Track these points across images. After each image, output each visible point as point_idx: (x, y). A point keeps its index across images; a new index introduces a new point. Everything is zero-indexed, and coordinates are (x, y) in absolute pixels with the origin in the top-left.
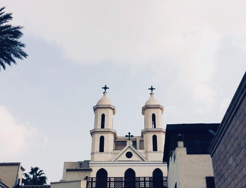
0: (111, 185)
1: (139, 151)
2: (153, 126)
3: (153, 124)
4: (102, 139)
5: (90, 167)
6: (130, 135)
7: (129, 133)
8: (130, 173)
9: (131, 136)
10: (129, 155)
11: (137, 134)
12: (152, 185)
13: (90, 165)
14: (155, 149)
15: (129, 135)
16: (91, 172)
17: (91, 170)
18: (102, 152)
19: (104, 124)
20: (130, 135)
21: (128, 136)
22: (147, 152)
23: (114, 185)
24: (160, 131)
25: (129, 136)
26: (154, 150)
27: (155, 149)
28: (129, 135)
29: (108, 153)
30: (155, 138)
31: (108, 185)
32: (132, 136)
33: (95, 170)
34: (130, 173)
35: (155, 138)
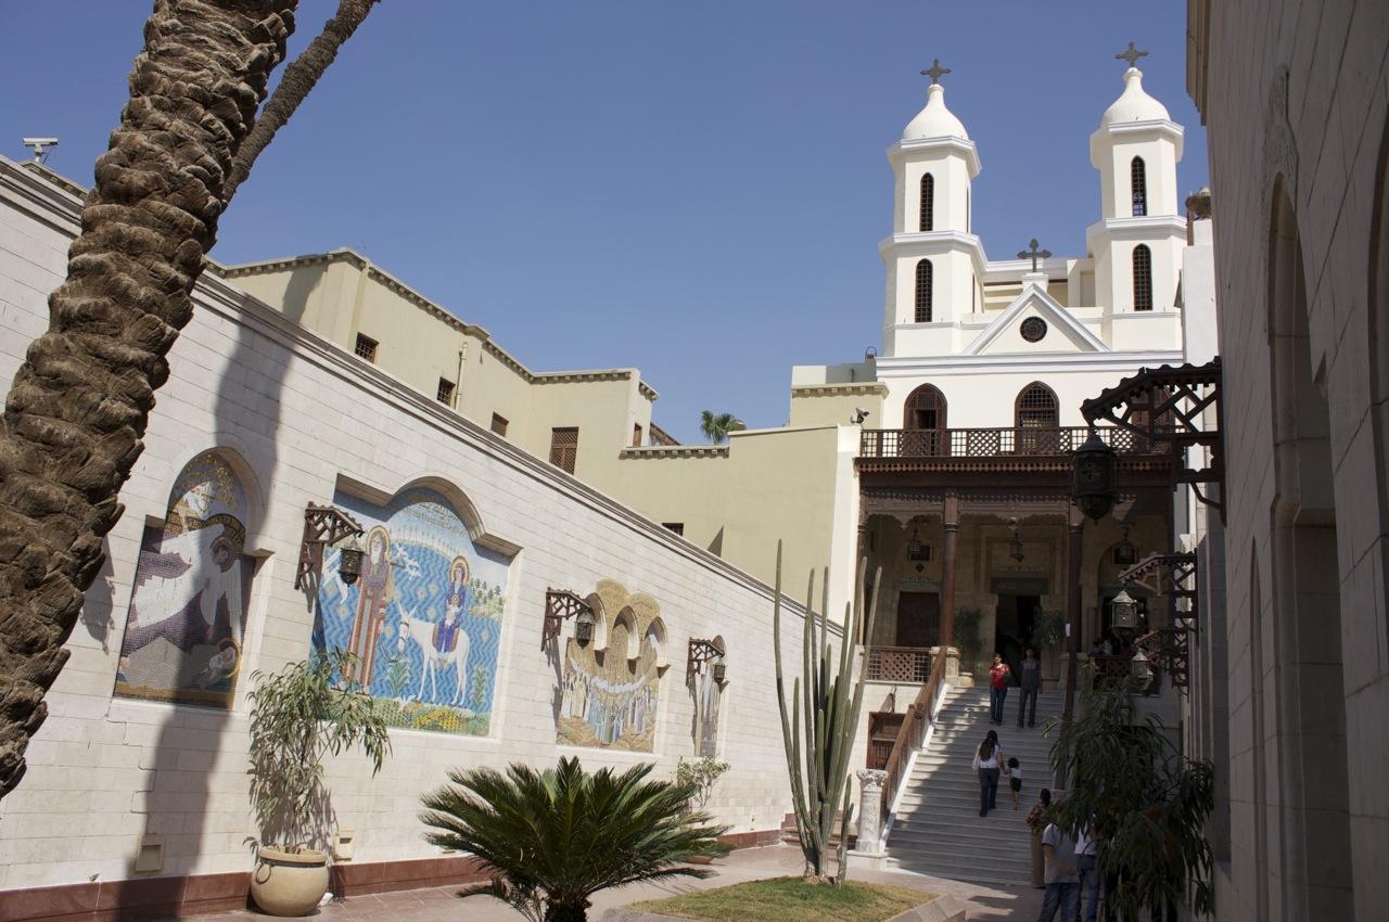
1: (1078, 313)
5: (880, 380)
6: (1039, 250)
7: (1034, 244)
8: (1037, 403)
10: (1033, 330)
13: (879, 373)
14: (1143, 300)
16: (885, 397)
17: (881, 391)
18: (924, 320)
22: (1106, 322)
23: (964, 442)
26: (1137, 308)
27: (1143, 300)
29: (950, 325)
34: (1037, 403)
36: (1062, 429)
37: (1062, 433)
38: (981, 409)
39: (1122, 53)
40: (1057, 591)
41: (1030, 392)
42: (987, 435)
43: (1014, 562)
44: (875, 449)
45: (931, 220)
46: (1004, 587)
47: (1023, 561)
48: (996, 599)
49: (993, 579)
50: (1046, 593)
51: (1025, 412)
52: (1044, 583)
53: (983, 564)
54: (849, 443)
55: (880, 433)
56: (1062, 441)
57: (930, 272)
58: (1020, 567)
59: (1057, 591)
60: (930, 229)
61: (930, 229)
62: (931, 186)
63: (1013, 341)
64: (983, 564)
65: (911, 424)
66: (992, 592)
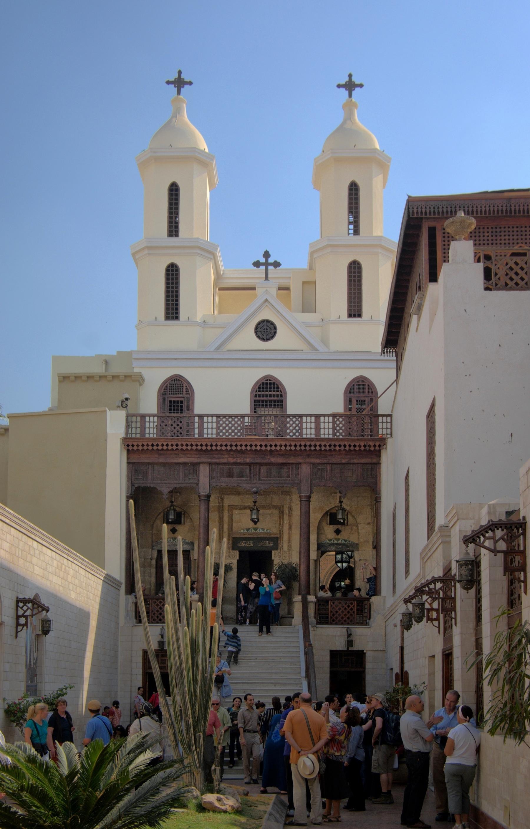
0: (205, 425)
2: (351, 227)
3: (350, 223)
4: (172, 273)
6: (271, 260)
7: (267, 255)
9: (271, 264)
10: (266, 330)
11: (294, 259)
12: (341, 429)
15: (267, 260)
16: (141, 385)
19: (177, 223)
20: (271, 260)
21: (262, 264)
24: (378, 245)
25: (267, 264)
26: (350, 316)
28: (267, 260)
30: (355, 271)
31: (196, 425)
32: (277, 264)
33: (155, 377)
35: (355, 271)
36: (289, 416)
37: (288, 420)
38: (222, 396)
39: (343, 83)
40: (286, 548)
41: (263, 384)
42: (227, 420)
43: (251, 525)
44: (138, 431)
45: (177, 227)
46: (243, 545)
47: (258, 523)
48: (237, 553)
49: (233, 538)
50: (277, 549)
51: (259, 401)
52: (275, 541)
53: (226, 527)
54: (115, 425)
55: (143, 416)
56: (288, 425)
57: (177, 275)
58: (256, 529)
59: (286, 548)
60: (177, 235)
61: (177, 235)
62: (177, 195)
63: (248, 339)
64: (226, 527)
65: (164, 409)
66: (234, 549)
